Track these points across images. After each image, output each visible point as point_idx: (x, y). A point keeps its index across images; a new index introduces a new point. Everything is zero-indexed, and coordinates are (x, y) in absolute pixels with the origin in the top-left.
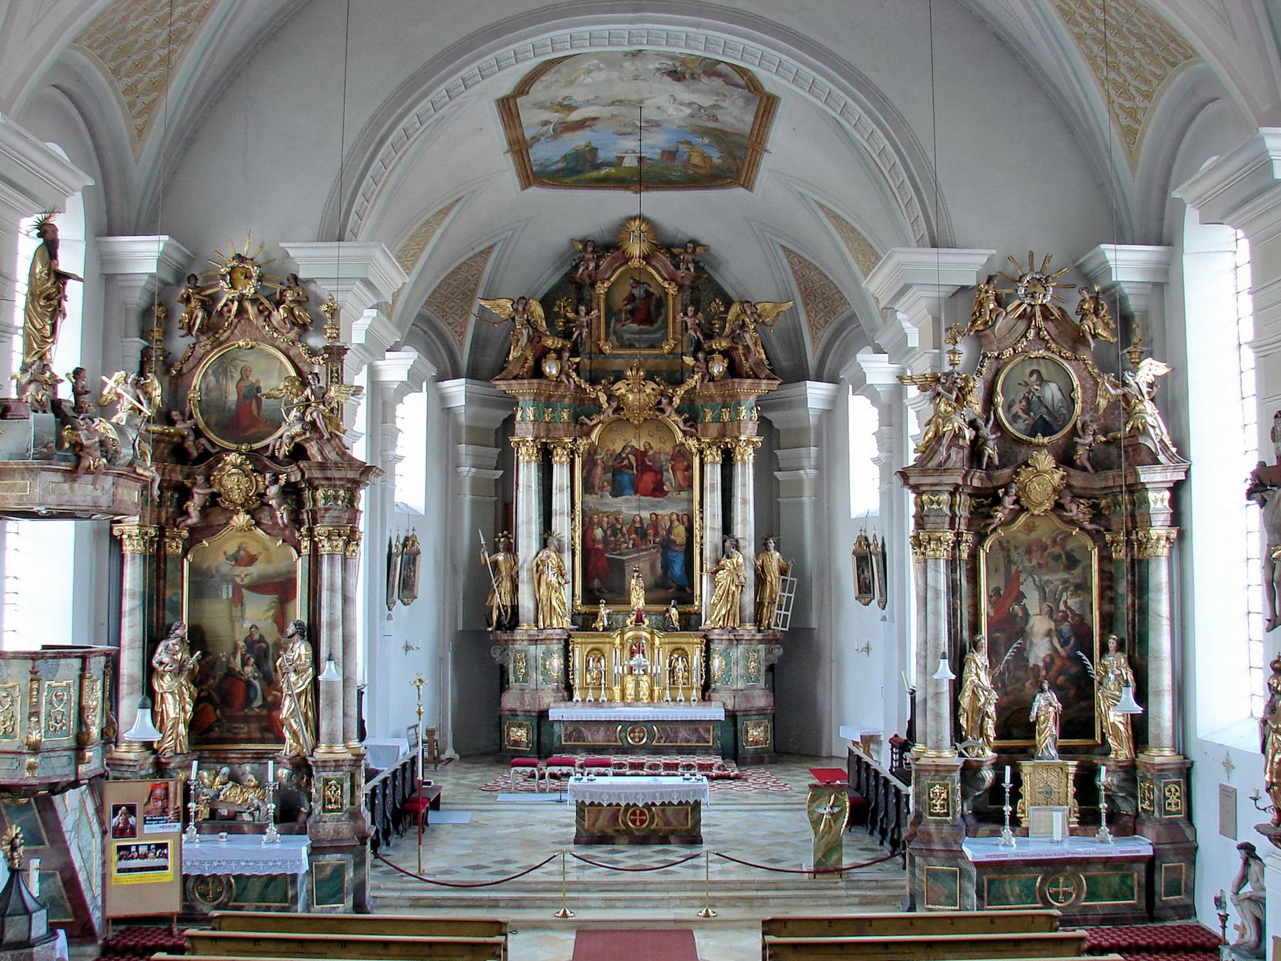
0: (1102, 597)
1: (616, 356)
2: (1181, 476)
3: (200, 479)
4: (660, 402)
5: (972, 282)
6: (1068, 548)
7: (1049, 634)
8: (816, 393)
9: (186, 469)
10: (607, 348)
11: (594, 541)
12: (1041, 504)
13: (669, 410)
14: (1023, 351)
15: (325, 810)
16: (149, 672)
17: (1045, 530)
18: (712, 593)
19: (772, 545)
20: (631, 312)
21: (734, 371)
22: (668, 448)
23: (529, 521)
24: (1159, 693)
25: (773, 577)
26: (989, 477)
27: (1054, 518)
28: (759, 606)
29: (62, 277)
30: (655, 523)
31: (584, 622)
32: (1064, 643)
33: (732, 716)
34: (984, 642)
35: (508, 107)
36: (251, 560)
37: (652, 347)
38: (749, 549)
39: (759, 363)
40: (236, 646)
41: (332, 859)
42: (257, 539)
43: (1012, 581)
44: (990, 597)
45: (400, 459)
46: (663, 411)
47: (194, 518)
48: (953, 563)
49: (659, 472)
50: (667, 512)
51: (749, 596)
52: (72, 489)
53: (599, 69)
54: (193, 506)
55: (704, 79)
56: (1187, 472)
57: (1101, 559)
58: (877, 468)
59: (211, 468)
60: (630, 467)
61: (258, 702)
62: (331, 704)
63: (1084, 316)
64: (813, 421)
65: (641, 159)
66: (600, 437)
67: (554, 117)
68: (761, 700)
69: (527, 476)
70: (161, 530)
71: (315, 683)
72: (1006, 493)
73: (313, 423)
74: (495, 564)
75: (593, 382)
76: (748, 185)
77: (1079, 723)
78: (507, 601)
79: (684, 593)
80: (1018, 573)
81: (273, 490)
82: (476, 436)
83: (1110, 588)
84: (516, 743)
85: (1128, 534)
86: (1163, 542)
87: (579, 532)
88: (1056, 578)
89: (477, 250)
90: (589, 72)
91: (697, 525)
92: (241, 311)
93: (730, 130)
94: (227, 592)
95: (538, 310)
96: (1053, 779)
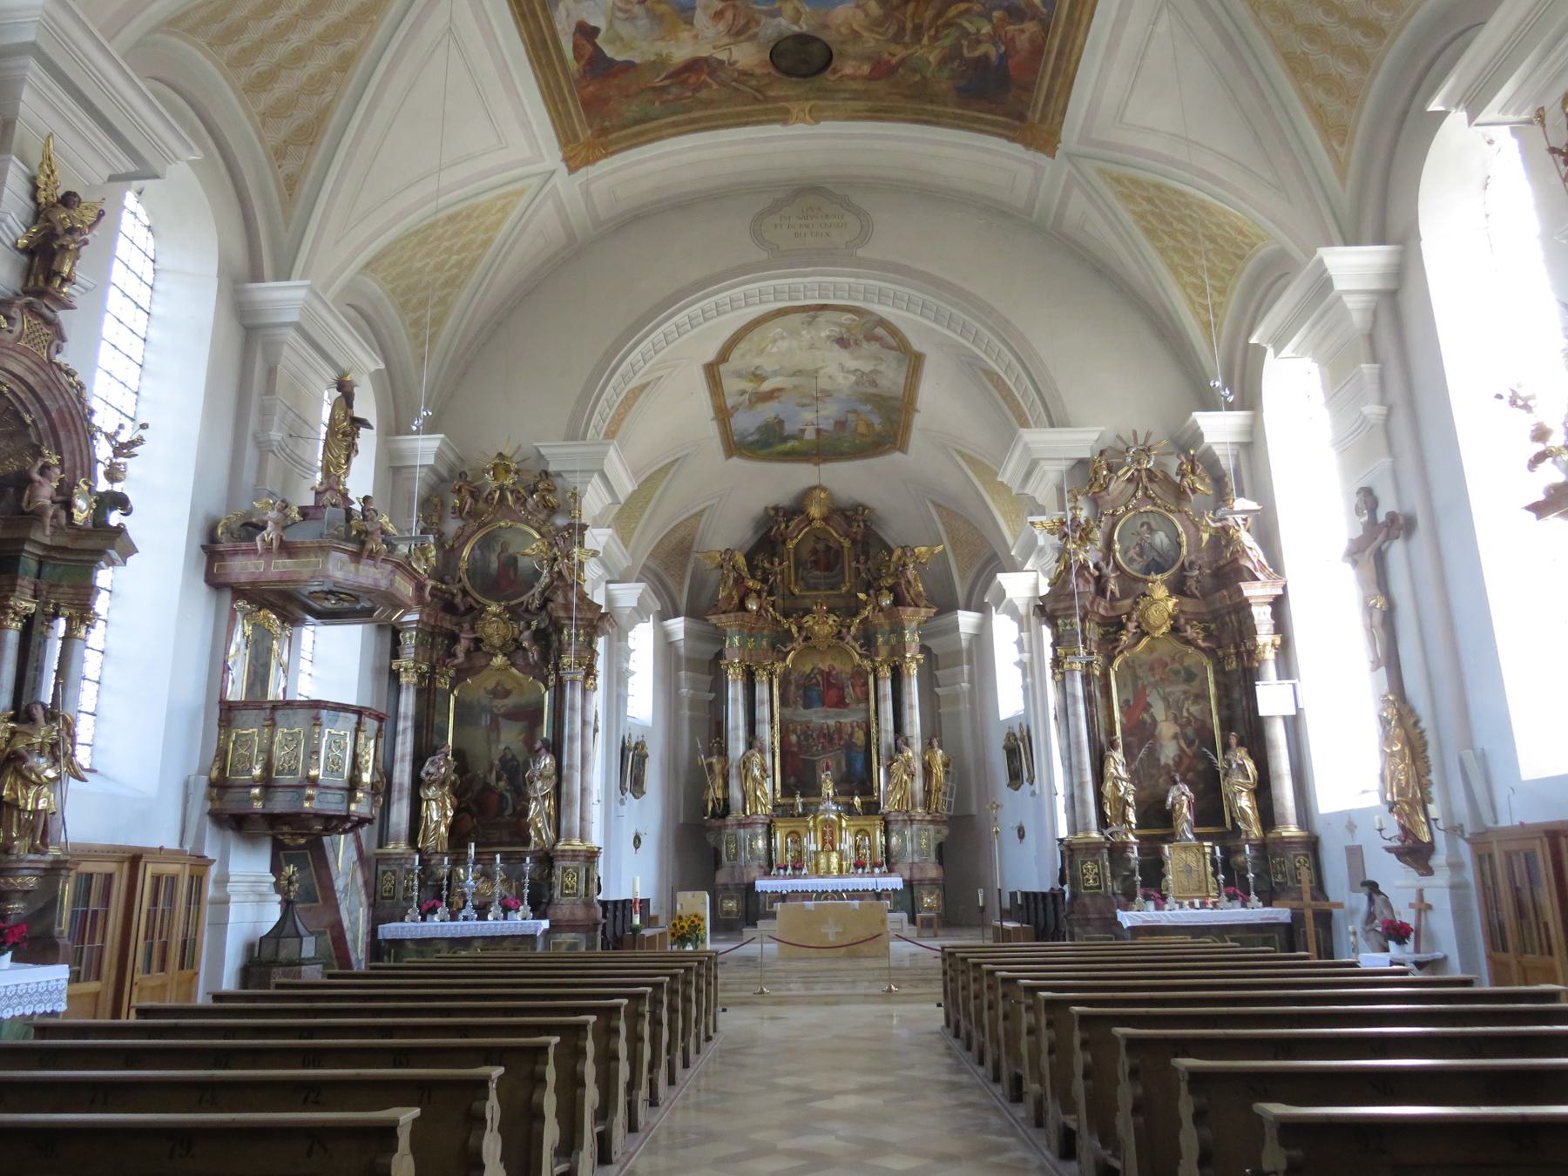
0: (1219, 704)
1: (803, 597)
2: (1280, 592)
3: (466, 626)
4: (840, 632)
5: (1087, 455)
6: (1186, 663)
7: (1175, 737)
8: (966, 620)
9: (455, 619)
10: (796, 591)
11: (790, 744)
12: (1160, 627)
13: (848, 638)
14: (1134, 508)
15: (563, 894)
16: (417, 782)
17: (1166, 649)
18: (887, 783)
19: (936, 743)
20: (816, 562)
21: (898, 601)
22: (848, 669)
23: (736, 728)
24: (1279, 777)
25: (938, 770)
26: (1113, 608)
27: (1171, 638)
28: (928, 793)
29: (360, 423)
30: (839, 728)
31: (783, 811)
32: (1190, 744)
33: (909, 884)
34: (1120, 741)
35: (712, 371)
36: (507, 694)
37: (832, 589)
38: (918, 746)
39: (919, 595)
40: (491, 766)
41: (567, 938)
42: (513, 677)
43: (1140, 694)
44: (1121, 707)
45: (633, 673)
46: (842, 639)
47: (461, 658)
48: (1087, 679)
49: (841, 689)
50: (848, 720)
51: (918, 784)
52: (357, 570)
54: (460, 649)
55: (865, 345)
56: (1285, 588)
57: (1216, 673)
58: (1019, 671)
59: (475, 619)
60: (818, 684)
61: (509, 811)
62: (570, 804)
63: (1183, 476)
64: (964, 644)
65: (818, 431)
66: (793, 661)
67: (748, 386)
68: (933, 872)
69: (735, 691)
70: (432, 668)
71: (558, 788)
72: (1129, 619)
73: (560, 573)
74: (710, 766)
75: (786, 616)
76: (903, 448)
77: (1212, 810)
78: (719, 794)
79: (864, 785)
80: (1144, 687)
81: (526, 634)
82: (693, 664)
83: (1227, 696)
84: (729, 913)
85: (1237, 647)
86: (1269, 648)
87: (777, 738)
88: (1177, 690)
89: (692, 512)
90: (775, 341)
91: (873, 730)
92: (503, 498)
94: (485, 720)
95: (741, 560)
96: (1191, 859)
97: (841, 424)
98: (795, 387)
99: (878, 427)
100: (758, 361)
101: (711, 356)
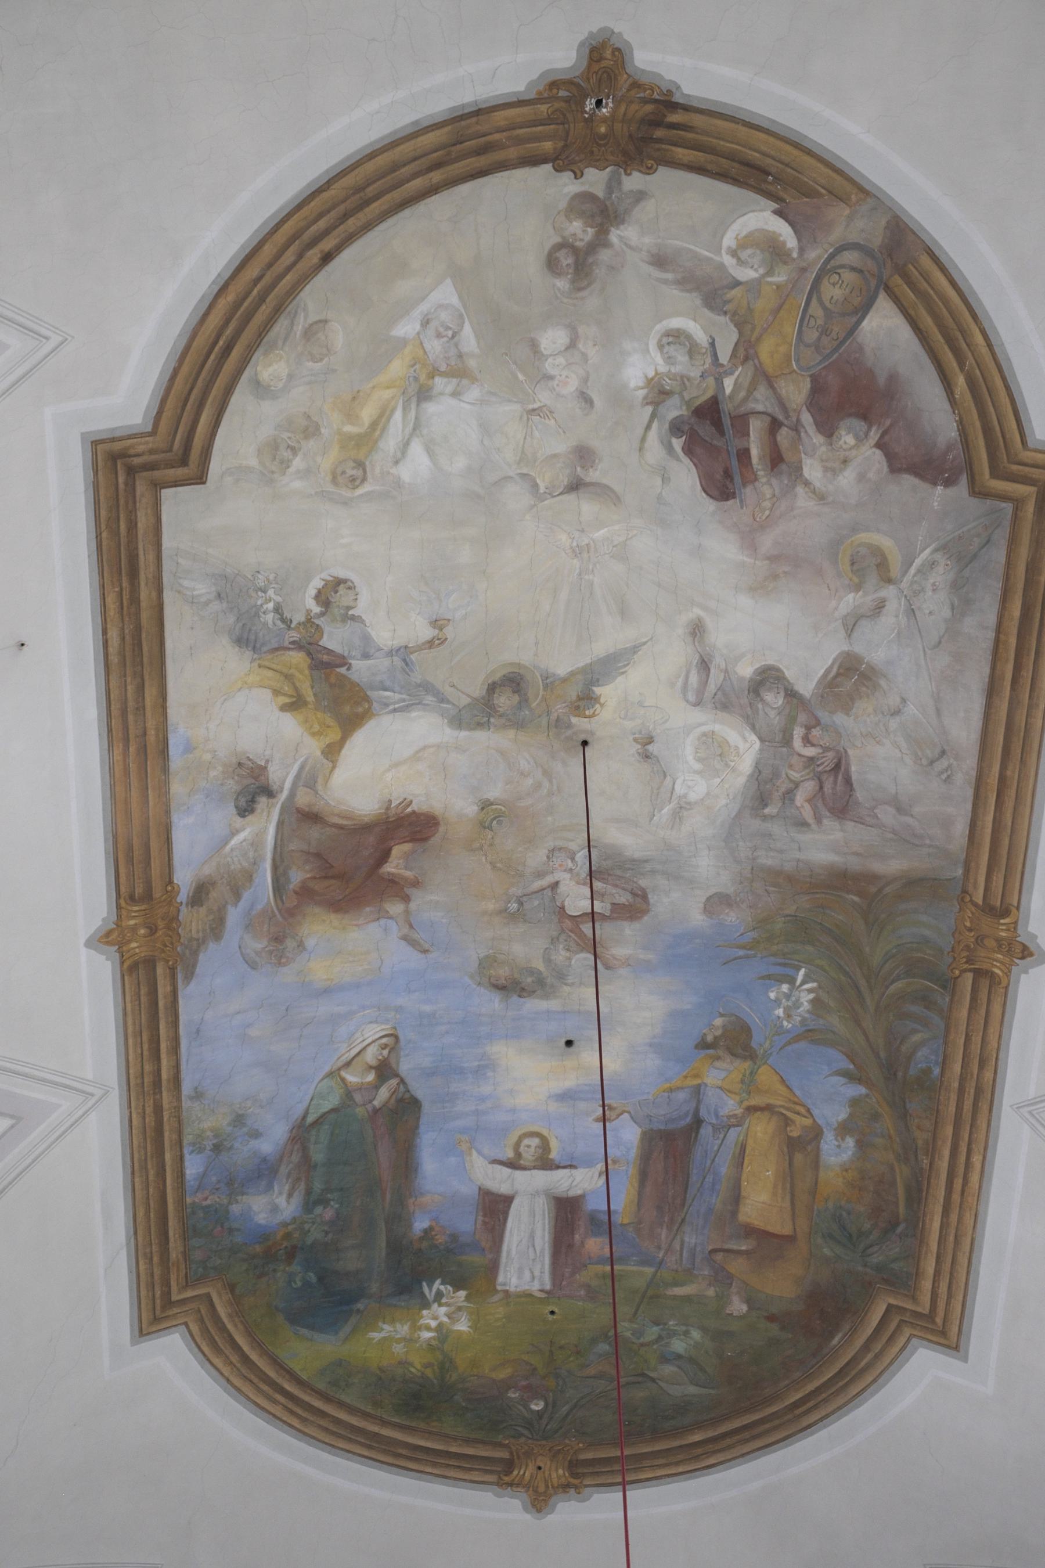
53: (459, 372)
76: (946, 1330)
93: (893, 866)
97: (672, 1148)
98: (491, 816)
99: (837, 1153)
100: (343, 541)
101: (127, 399)
